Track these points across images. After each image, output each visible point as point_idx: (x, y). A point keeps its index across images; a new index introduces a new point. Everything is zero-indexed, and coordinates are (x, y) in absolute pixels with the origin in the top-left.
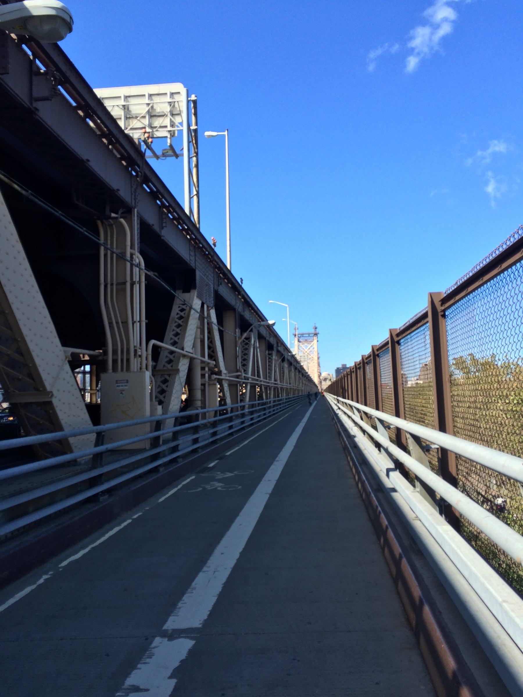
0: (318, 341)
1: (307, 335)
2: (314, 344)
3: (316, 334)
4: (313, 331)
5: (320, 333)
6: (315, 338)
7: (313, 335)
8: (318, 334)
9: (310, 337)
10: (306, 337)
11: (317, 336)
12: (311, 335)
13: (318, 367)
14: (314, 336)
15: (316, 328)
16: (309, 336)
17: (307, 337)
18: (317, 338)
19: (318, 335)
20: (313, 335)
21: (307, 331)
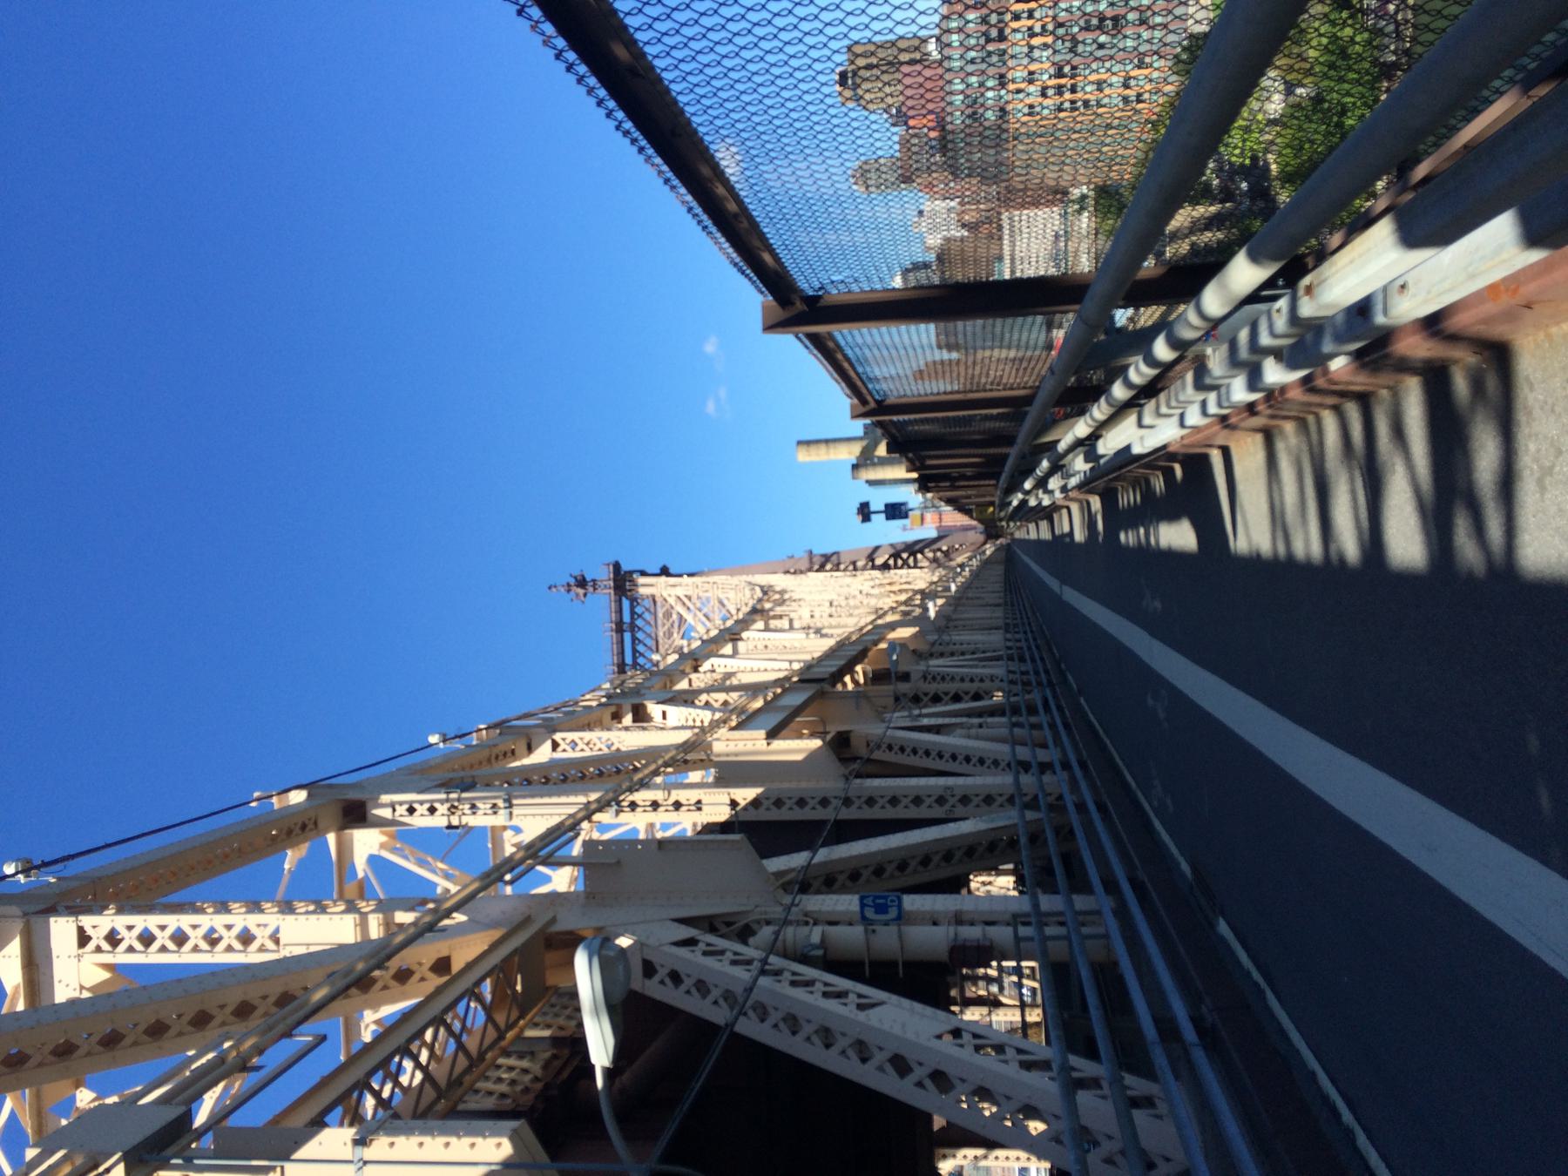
0: (665, 572)
1: (627, 636)
2: (680, 592)
3: (623, 582)
4: (603, 599)
5: (612, 560)
6: (648, 587)
7: (626, 603)
8: (617, 566)
9: (639, 622)
10: (640, 648)
11: (631, 573)
12: (627, 618)
13: (836, 568)
14: (634, 601)
15: (582, 582)
16: (633, 628)
17: (634, 639)
18: (643, 573)
19: (625, 567)
20: (624, 599)
21: (608, 636)
